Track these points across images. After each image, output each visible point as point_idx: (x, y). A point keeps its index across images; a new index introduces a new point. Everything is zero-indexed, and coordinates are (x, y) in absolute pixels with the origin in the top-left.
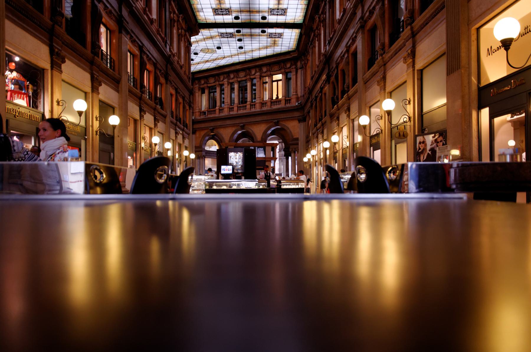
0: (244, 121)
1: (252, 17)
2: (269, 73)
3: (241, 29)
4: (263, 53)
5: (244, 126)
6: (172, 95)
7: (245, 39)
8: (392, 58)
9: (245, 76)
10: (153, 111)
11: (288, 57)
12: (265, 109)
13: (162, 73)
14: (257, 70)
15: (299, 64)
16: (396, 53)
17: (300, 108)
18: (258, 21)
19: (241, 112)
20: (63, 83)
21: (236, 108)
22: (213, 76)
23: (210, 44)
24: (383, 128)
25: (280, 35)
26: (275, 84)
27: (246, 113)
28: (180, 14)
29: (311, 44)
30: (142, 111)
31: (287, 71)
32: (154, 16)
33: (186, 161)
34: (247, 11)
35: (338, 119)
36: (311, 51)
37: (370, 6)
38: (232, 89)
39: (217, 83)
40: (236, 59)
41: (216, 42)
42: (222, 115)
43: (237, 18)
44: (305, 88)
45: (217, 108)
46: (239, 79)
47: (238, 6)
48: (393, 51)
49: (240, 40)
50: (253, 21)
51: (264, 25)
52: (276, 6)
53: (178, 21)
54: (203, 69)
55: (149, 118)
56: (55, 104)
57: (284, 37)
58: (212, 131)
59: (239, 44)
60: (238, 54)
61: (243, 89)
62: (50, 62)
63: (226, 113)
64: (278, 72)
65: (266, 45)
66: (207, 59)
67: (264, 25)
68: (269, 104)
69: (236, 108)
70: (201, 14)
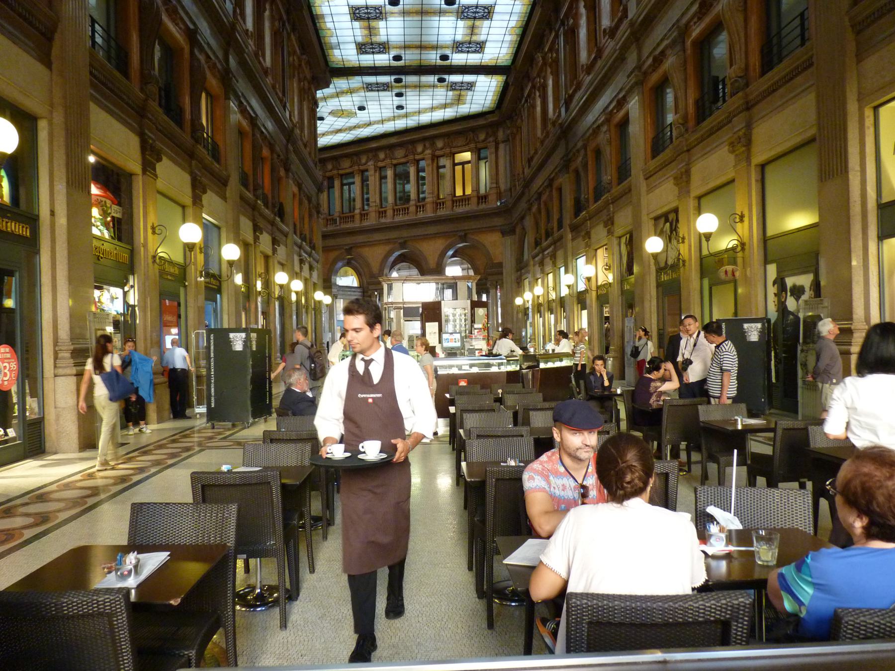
0: (405, 233)
1: (423, 57)
2: (448, 150)
3: (403, 77)
4: (439, 115)
5: (405, 242)
6: (294, 195)
7: (408, 94)
8: (702, 141)
9: (406, 156)
10: (270, 227)
11: (481, 122)
12: (442, 212)
13: (282, 160)
14: (427, 145)
15: (501, 135)
16: (712, 132)
17: (504, 211)
18: (433, 62)
19: (400, 218)
20: (159, 196)
21: (390, 213)
22: (346, 156)
23: (347, 102)
24: (686, 258)
25: (471, 86)
26: (458, 168)
27: (408, 220)
28: (302, 54)
29: (526, 101)
30: (256, 229)
31: (479, 146)
32: (268, 61)
33: (314, 309)
34: (416, 47)
35: (588, 235)
36: (525, 114)
37: (655, 49)
38: (383, 178)
39: (356, 168)
40: (390, 127)
41: (357, 99)
42: (366, 223)
43: (397, 58)
44: (513, 175)
45: (357, 211)
46: (395, 162)
47: (401, 38)
48: (704, 130)
49: (399, 95)
50: (424, 63)
51: (443, 70)
52: (467, 38)
53: (300, 65)
54: (330, 144)
55: (265, 239)
56: (150, 231)
57: (477, 89)
58: (349, 251)
59: (397, 101)
60: (394, 118)
61: (403, 177)
62: (140, 162)
63: (372, 220)
64: (464, 149)
65: (444, 102)
66: (339, 127)
67: (443, 70)
68: (449, 203)
69: (390, 213)
70: (336, 52)
